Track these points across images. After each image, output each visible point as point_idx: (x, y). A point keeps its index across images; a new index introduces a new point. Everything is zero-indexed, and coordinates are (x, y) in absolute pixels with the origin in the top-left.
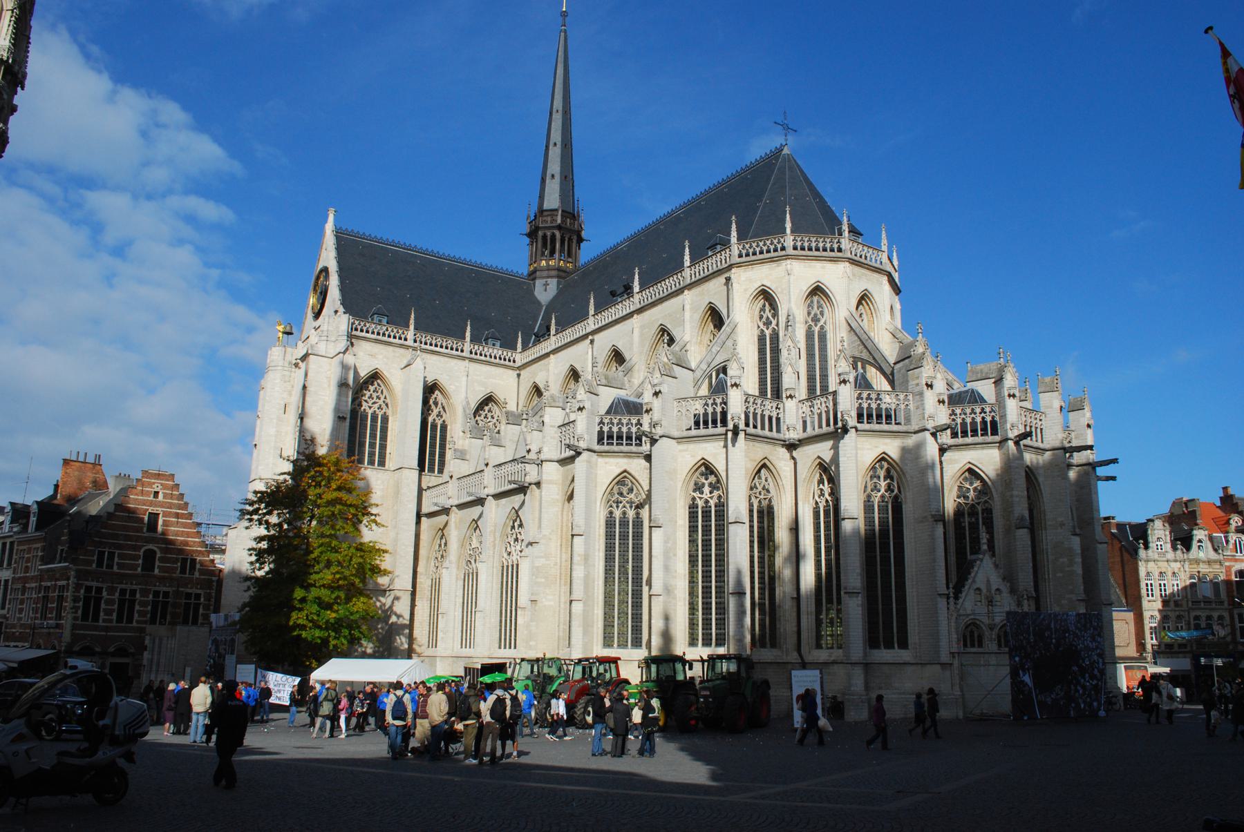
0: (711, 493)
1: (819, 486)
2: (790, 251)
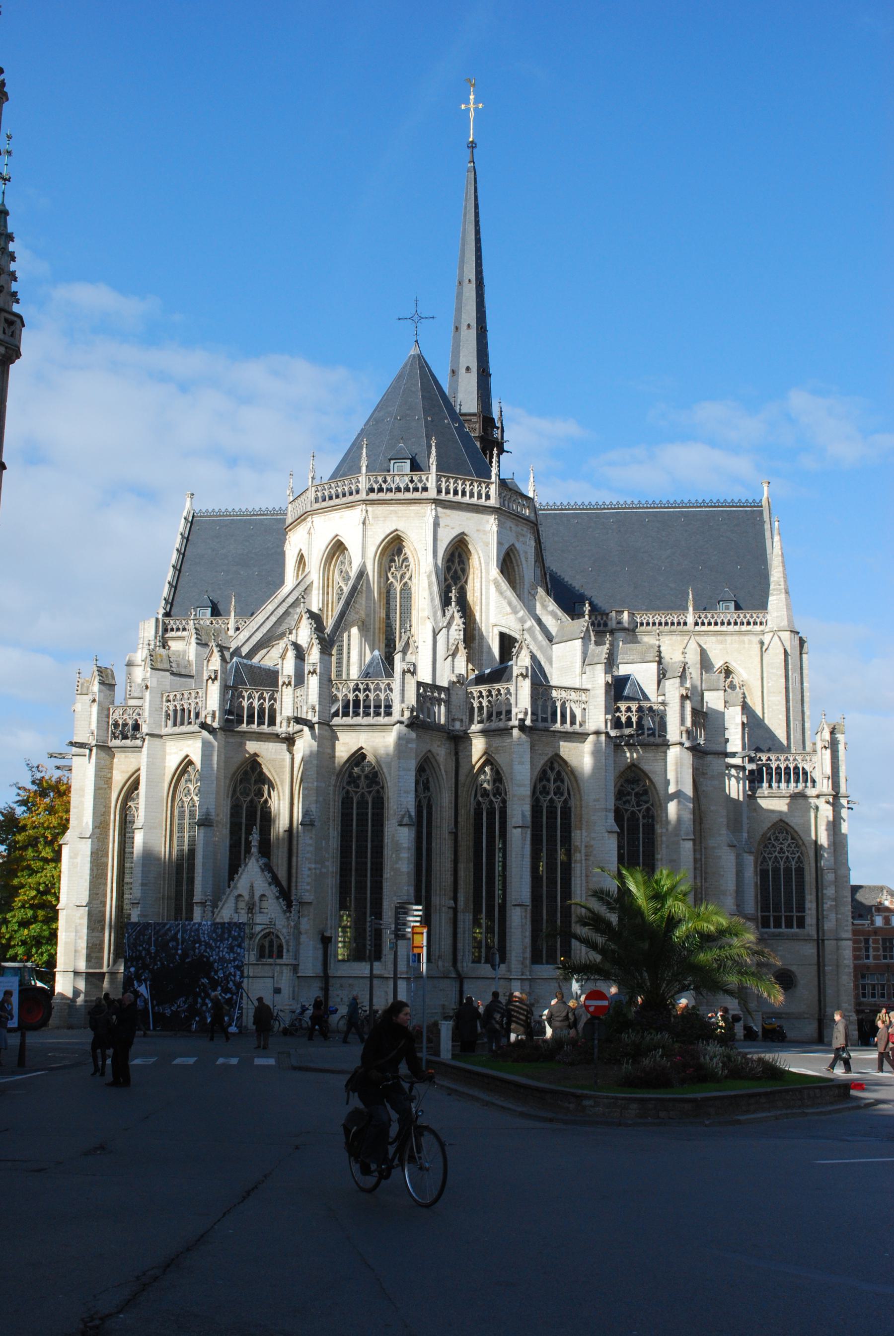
0: (369, 786)
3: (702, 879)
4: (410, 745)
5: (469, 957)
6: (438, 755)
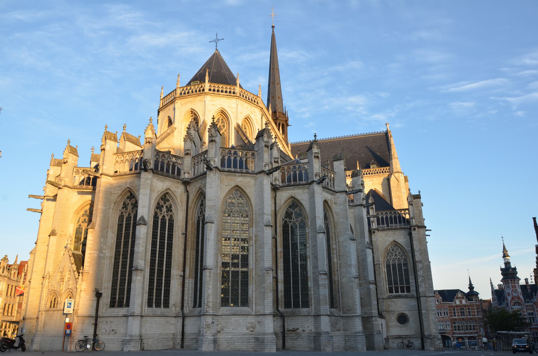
0: (132, 209)
1: (201, 206)
3: (337, 259)
5: (191, 304)
6: (175, 192)
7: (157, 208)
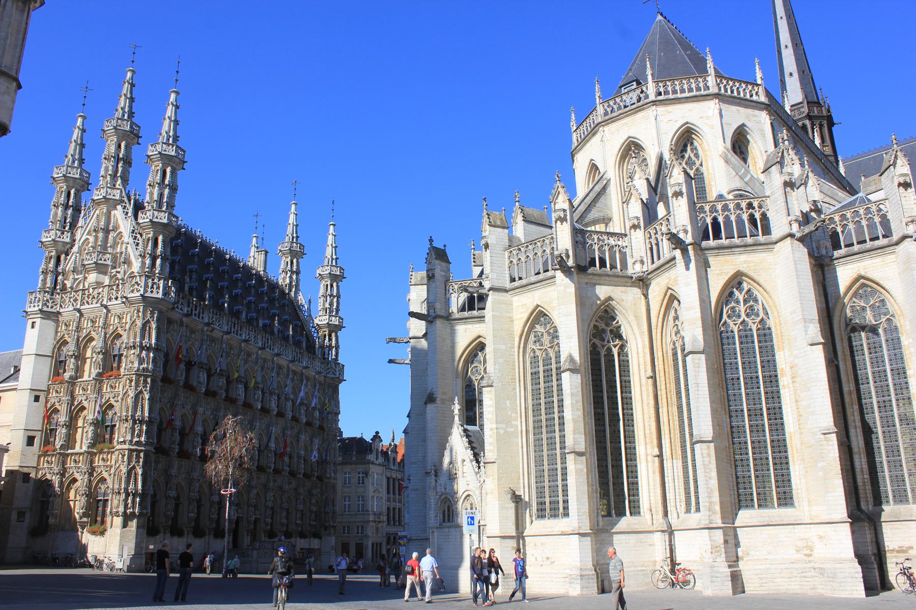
0: (551, 342)
2: (652, 97)
4: (568, 290)
5: (682, 507)
6: (623, 301)
7: (594, 336)
